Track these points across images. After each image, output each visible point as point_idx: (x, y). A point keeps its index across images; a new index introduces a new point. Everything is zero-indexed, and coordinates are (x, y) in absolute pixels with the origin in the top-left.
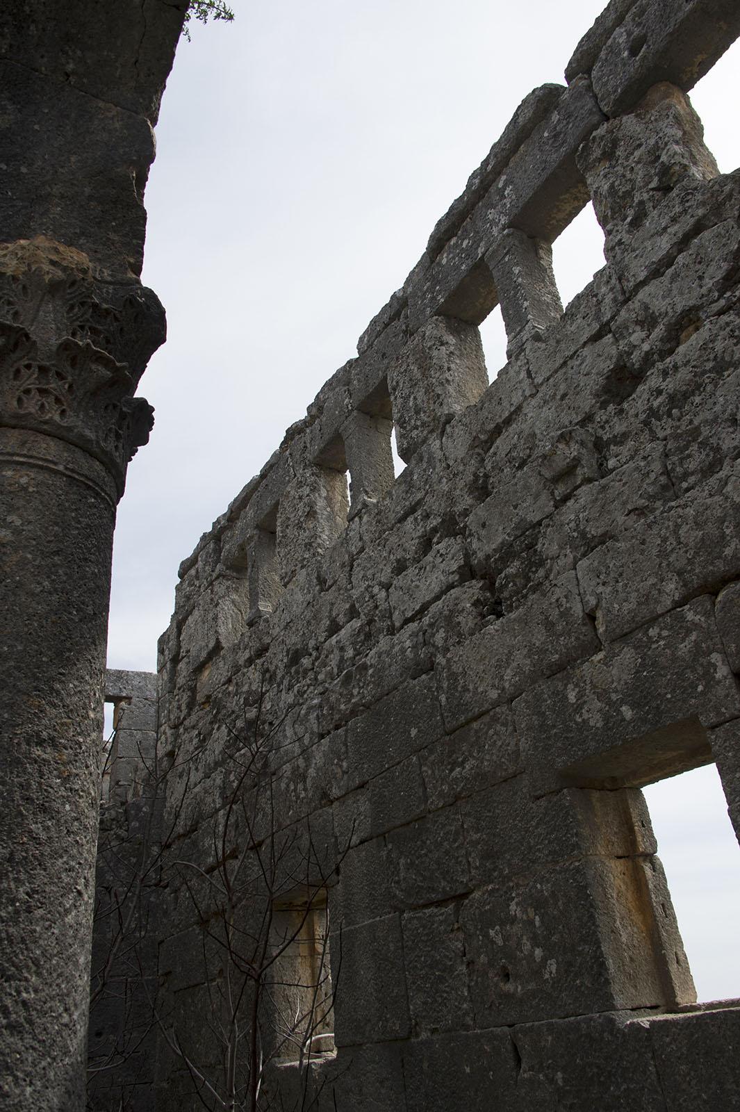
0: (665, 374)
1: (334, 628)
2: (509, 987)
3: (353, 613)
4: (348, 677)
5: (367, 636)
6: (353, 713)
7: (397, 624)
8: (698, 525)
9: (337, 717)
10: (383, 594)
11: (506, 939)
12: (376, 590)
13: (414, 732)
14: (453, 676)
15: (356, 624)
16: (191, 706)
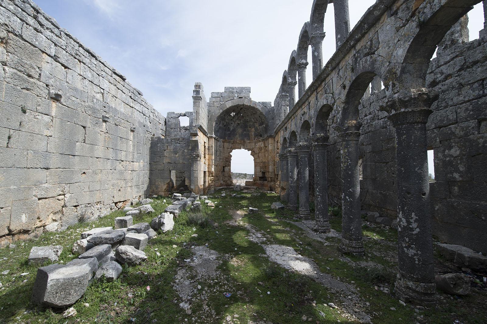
0: (443, 85)
1: (366, 116)
2: (394, 175)
3: (370, 114)
4: (369, 125)
5: (373, 119)
6: (369, 132)
7: (380, 118)
8: (440, 117)
9: (366, 132)
10: (377, 112)
11: (394, 169)
12: (376, 111)
13: (381, 138)
14: (390, 130)
15: (371, 116)
16: (333, 122)
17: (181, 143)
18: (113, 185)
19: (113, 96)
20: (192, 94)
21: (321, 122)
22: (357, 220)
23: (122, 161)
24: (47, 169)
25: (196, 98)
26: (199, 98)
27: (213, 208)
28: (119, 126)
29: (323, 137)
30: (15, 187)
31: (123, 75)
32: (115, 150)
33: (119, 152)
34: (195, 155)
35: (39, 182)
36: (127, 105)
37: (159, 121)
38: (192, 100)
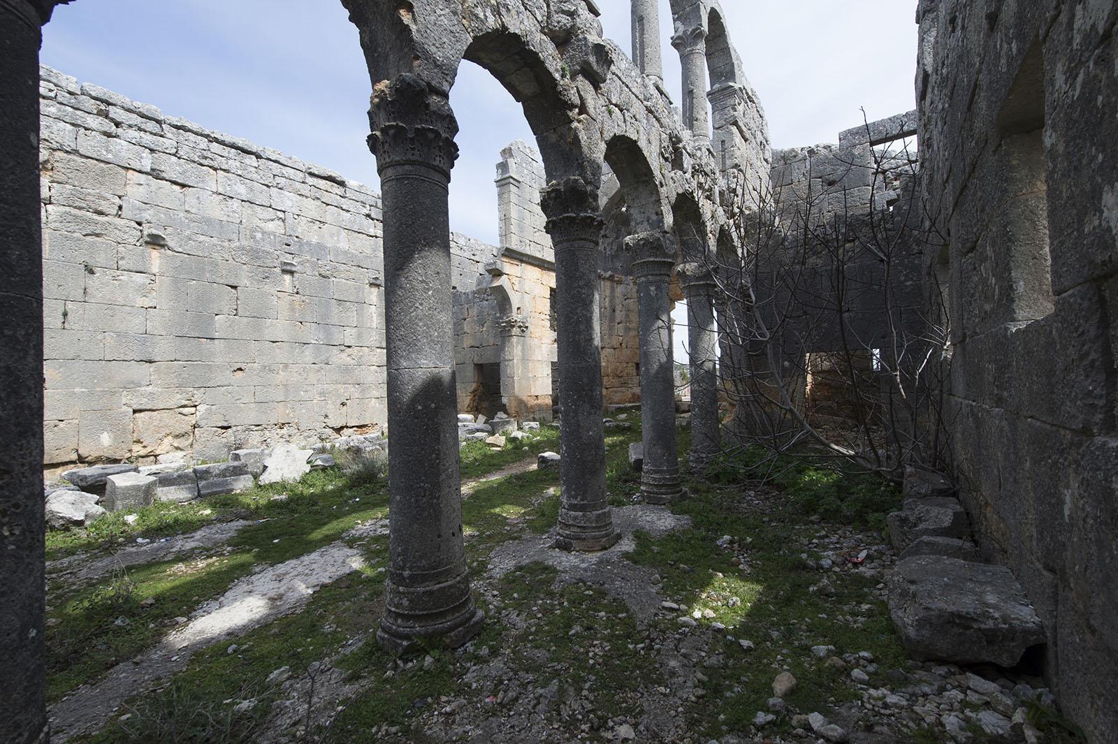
17: (489, 298)
18: (322, 394)
19: (313, 221)
20: (494, 175)
21: (553, 138)
22: (398, 498)
23: (349, 347)
24: (151, 362)
25: (503, 182)
26: (507, 181)
27: (499, 449)
28: (334, 279)
29: (553, 195)
30: (84, 390)
31: (334, 175)
32: (324, 324)
33: (334, 329)
34: (506, 322)
35: (133, 382)
36: (359, 233)
37: (473, 257)
38: (495, 190)
